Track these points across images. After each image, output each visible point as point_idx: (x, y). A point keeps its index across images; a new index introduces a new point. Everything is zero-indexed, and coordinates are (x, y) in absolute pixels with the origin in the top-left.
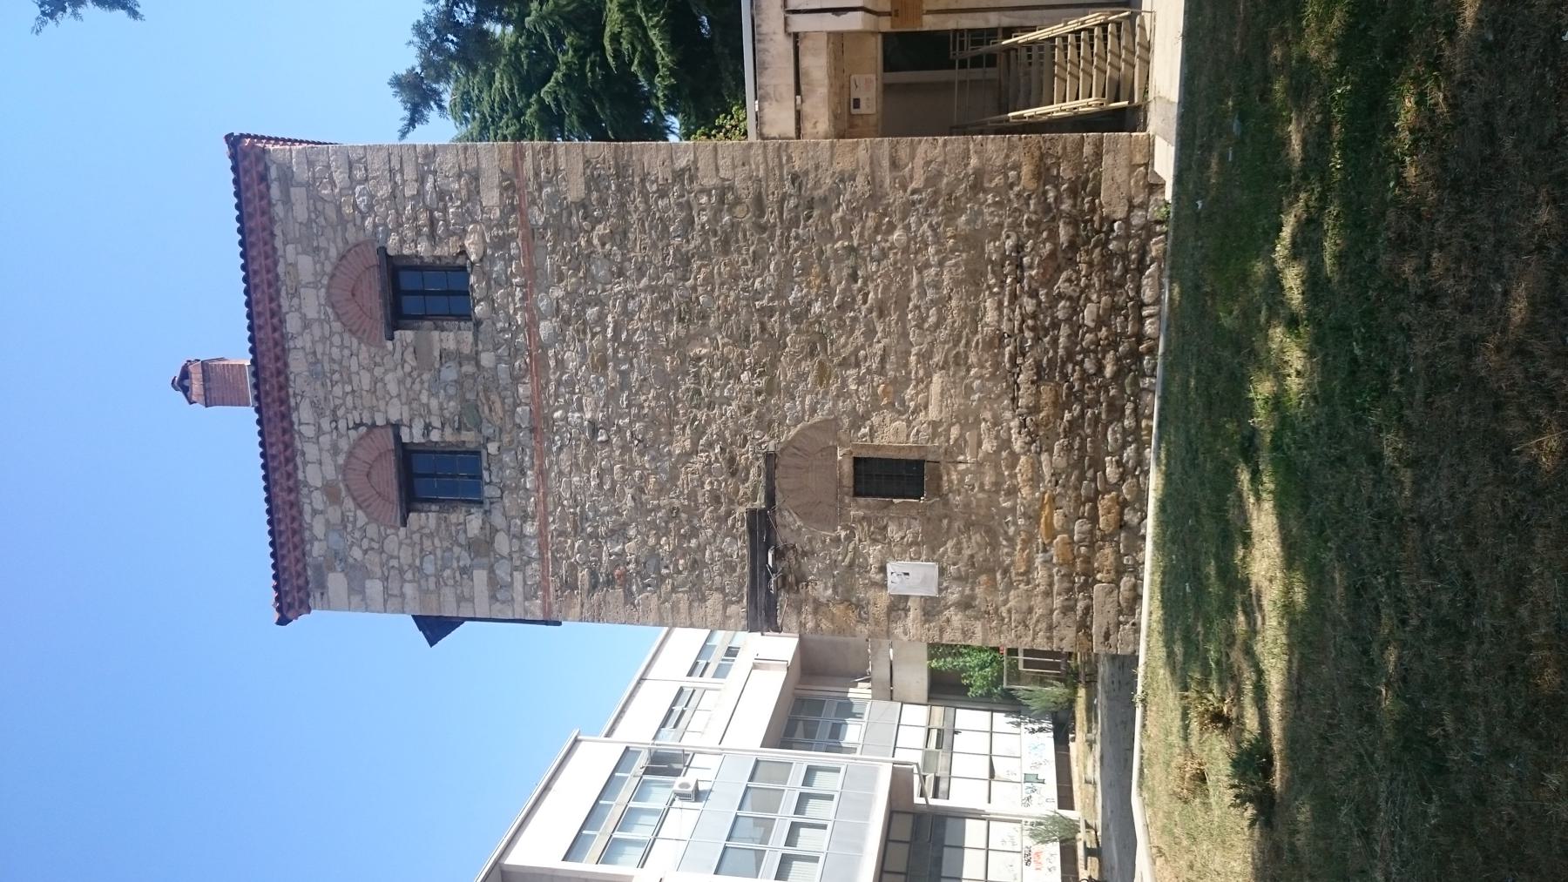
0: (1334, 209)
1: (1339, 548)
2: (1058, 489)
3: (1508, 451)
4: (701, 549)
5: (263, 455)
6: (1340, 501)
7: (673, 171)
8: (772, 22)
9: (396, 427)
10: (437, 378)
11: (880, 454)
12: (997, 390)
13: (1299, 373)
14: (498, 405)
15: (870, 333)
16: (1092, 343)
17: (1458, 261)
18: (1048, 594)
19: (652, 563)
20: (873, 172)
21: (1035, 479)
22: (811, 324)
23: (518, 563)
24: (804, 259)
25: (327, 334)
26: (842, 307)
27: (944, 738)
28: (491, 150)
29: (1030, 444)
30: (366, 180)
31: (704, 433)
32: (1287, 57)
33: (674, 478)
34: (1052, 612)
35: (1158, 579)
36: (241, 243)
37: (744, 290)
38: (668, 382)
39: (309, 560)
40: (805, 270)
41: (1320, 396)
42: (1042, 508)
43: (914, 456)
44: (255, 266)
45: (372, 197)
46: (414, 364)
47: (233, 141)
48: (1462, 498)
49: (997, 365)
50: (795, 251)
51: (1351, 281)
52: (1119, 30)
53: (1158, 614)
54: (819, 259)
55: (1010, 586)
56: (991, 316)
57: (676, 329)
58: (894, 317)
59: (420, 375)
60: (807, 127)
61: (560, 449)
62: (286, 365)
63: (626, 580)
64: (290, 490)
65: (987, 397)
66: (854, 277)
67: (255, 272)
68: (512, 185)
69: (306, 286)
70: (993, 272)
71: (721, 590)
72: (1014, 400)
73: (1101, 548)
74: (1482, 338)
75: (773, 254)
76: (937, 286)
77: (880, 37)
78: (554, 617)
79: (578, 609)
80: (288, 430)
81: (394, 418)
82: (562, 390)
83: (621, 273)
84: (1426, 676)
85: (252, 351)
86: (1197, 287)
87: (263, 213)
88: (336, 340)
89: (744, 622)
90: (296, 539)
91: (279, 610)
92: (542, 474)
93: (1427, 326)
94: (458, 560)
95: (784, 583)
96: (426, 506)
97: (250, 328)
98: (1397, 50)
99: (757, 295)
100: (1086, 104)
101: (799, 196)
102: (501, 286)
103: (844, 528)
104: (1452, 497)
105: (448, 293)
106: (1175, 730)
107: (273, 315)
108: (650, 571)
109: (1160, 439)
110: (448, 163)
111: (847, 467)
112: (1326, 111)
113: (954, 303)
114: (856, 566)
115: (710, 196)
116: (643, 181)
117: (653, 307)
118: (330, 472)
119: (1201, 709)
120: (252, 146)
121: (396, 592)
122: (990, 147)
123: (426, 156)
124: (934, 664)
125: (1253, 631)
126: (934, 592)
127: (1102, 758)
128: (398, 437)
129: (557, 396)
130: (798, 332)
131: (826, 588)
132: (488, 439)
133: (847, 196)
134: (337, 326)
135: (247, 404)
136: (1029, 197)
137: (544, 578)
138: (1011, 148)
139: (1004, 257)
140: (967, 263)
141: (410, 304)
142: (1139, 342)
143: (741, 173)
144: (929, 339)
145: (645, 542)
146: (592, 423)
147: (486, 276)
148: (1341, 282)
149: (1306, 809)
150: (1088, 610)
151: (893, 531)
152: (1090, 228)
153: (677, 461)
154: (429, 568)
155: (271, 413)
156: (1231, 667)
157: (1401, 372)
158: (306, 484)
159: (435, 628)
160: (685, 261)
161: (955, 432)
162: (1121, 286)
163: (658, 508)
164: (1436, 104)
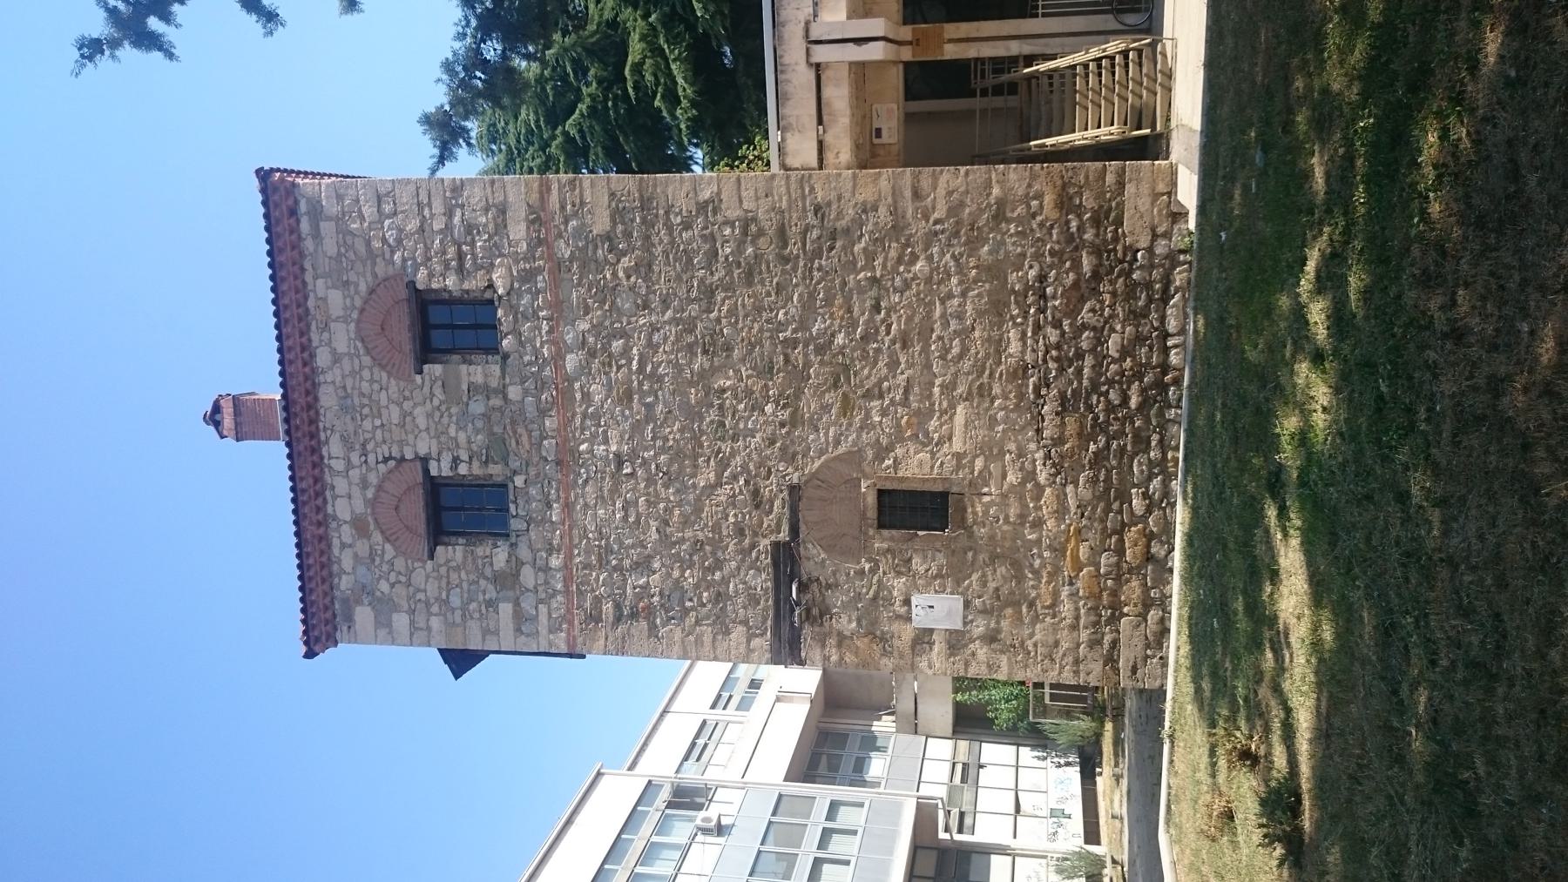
0: (1358, 244)
1: (1367, 586)
2: (1084, 522)
3: (1537, 492)
4: (725, 581)
5: (293, 489)
6: (1368, 539)
7: (697, 203)
8: (794, 52)
9: (425, 461)
10: (465, 413)
11: (904, 486)
12: (1022, 422)
13: (1325, 409)
14: (525, 439)
15: (893, 364)
16: (1117, 373)
17: (1484, 298)
18: (1074, 627)
19: (676, 596)
20: (895, 202)
21: (1061, 511)
22: (834, 356)
23: (543, 596)
24: (827, 290)
26: (865, 338)
27: (969, 772)
28: (517, 183)
29: (1055, 475)
30: (395, 214)
31: (728, 465)
32: (1309, 88)
33: (698, 510)
34: (1078, 645)
35: (1185, 612)
36: (272, 278)
37: (768, 321)
38: (693, 414)
39: (337, 593)
40: (829, 301)
41: (1346, 433)
42: (1068, 540)
43: (939, 488)
44: (286, 301)
45: (400, 230)
46: (442, 397)
47: (263, 175)
48: (1491, 539)
49: (1021, 396)
50: (818, 283)
51: (1376, 317)
52: (1140, 57)
53: (1186, 649)
54: (842, 290)
55: (1036, 619)
56: (1014, 347)
57: (700, 361)
58: (918, 348)
59: (448, 409)
60: (830, 157)
61: (586, 481)
62: (316, 399)
63: (650, 612)
64: (319, 524)
65: (1011, 429)
66: (877, 308)
67: (286, 307)
68: (538, 218)
69: (337, 320)
70: (1017, 302)
71: (745, 622)
72: (1039, 431)
73: (1128, 581)
74: (1509, 378)
75: (797, 285)
76: (960, 316)
77: (901, 67)
78: (578, 650)
79: (602, 642)
80: (318, 464)
81: (422, 452)
82: (588, 422)
83: (646, 306)
84: (1457, 718)
85: (283, 385)
86: (1222, 320)
87: (293, 248)
88: (366, 374)
89: (768, 655)
90: (325, 573)
91: (306, 643)
92: (568, 507)
93: (1454, 364)
94: (484, 592)
95: (807, 616)
96: (453, 539)
97: (281, 362)
98: (1419, 83)
99: (781, 327)
100: (1108, 133)
101: (822, 227)
102: (527, 319)
103: (869, 560)
104: (1481, 537)
105: (476, 327)
106: (1202, 766)
107: (303, 349)
108: (674, 604)
109: (1186, 472)
110: (475, 196)
111: (871, 499)
112: (1349, 143)
113: (977, 334)
114: (880, 599)
115: (733, 227)
116: (667, 213)
117: (677, 340)
118: (359, 506)
119: (1229, 746)
120: (282, 180)
121: (422, 624)
122: (1012, 176)
123: (454, 190)
124: (959, 697)
125: (1280, 669)
126: (959, 626)
127: (1129, 792)
128: (426, 471)
129: (583, 429)
130: (822, 363)
131: (850, 621)
132: (515, 473)
133: (870, 227)
134: (367, 360)
135: (271, 436)
136: (1052, 227)
137: (568, 611)
138: (1034, 177)
139: (1027, 288)
140: (990, 293)
141: (439, 338)
142: (1165, 373)
143: (764, 204)
144: (953, 370)
145: (669, 575)
146: (618, 455)
147: (513, 309)
148: (1366, 318)
149: (1336, 850)
150: (1115, 643)
151: (917, 564)
152: (1113, 258)
153: (702, 494)
154: (456, 601)
155: (301, 448)
156: (1258, 704)
157: (1430, 410)
158: (335, 518)
159: (460, 661)
160: (709, 292)
161: (979, 463)
162: (1146, 316)
163: (683, 540)
164: (1460, 139)
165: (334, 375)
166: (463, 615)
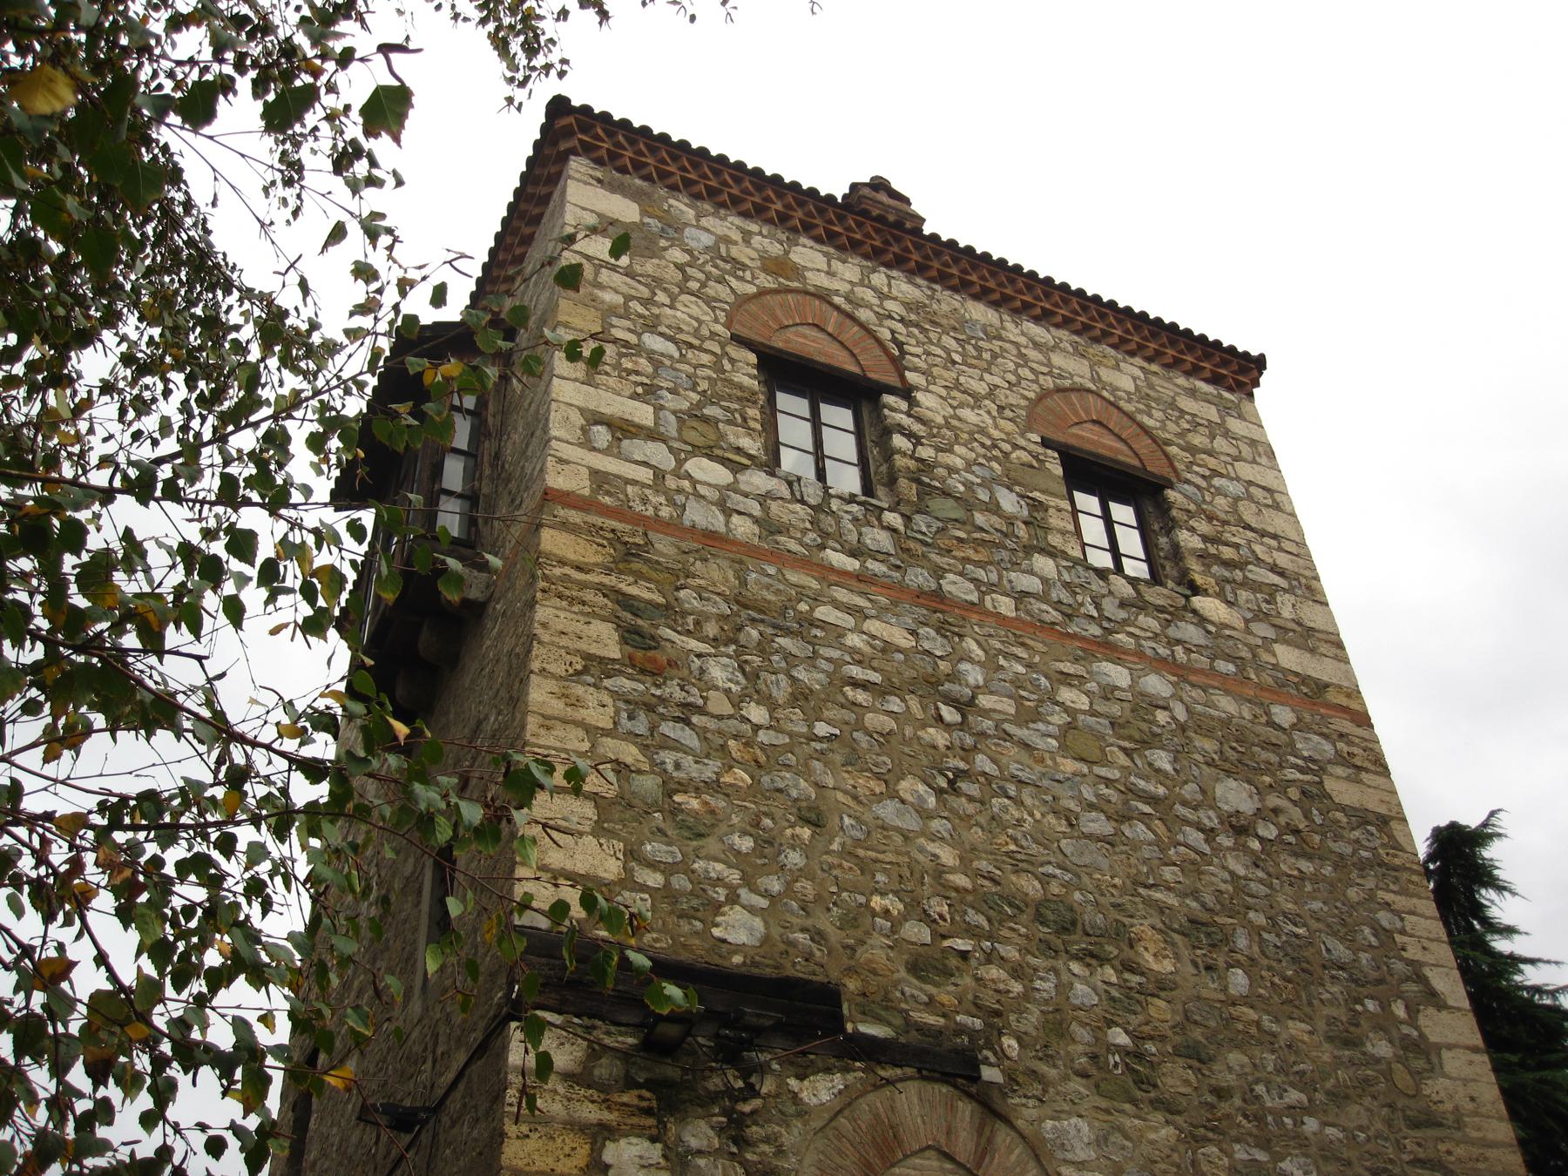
25: (1034, 366)
59: (995, 458)
62: (976, 297)
71: (628, 881)
118: (818, 280)
128: (892, 390)
132: (907, 519)
134: (1049, 383)
154: (654, 342)
165: (1012, 331)
166: (627, 344)
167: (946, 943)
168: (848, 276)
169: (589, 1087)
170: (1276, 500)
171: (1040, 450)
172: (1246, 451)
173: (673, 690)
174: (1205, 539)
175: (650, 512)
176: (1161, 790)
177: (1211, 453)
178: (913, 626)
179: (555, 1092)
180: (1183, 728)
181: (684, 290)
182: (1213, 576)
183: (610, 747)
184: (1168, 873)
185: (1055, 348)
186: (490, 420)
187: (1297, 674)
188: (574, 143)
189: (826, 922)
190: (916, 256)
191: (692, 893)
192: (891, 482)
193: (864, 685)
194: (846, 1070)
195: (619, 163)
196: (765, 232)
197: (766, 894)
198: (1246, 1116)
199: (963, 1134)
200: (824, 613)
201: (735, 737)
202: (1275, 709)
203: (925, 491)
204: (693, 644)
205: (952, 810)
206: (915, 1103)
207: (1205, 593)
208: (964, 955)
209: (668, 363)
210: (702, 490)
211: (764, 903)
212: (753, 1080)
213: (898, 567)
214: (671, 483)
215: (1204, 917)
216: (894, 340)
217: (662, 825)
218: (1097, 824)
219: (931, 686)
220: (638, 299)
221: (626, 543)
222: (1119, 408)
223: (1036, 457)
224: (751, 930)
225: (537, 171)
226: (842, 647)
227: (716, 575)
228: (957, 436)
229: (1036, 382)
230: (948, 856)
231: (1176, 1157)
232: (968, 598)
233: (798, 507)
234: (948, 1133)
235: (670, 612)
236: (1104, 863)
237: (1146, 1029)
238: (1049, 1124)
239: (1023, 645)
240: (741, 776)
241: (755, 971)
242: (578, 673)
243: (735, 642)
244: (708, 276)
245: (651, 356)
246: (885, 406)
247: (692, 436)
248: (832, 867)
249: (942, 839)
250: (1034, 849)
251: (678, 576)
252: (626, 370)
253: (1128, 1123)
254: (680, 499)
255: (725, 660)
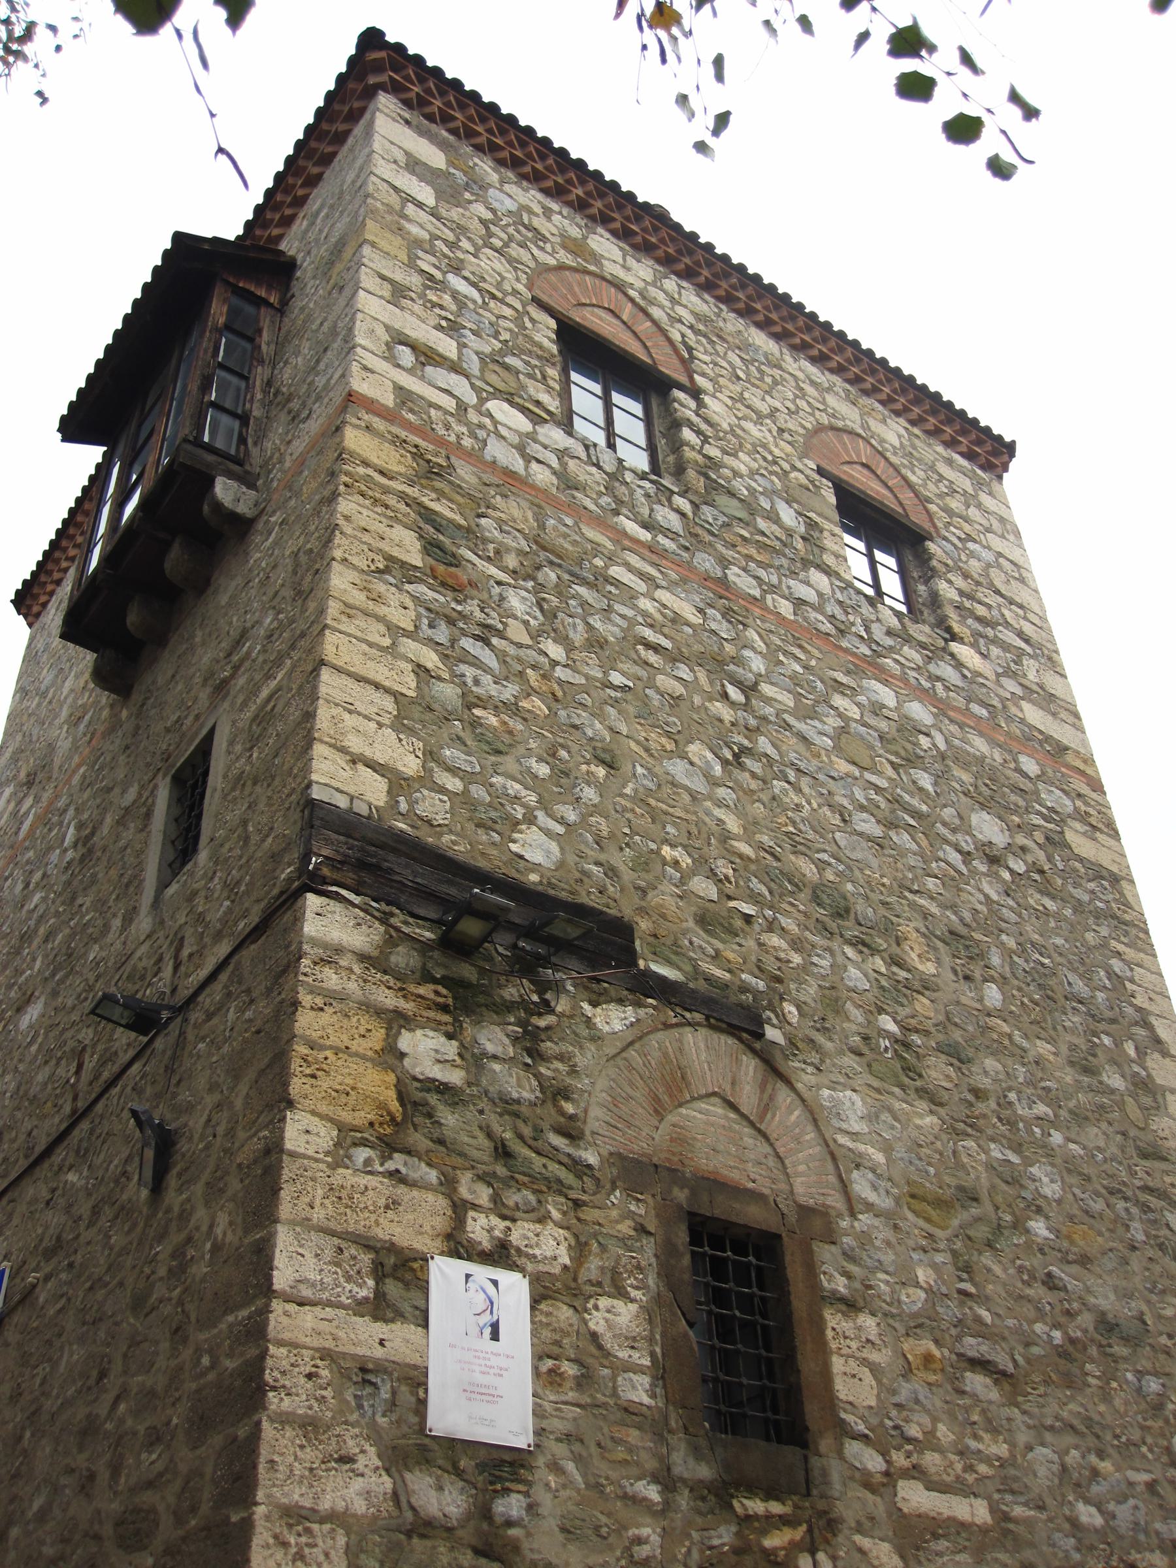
62: (759, 325)
71: (425, 780)
88: (802, 404)
118: (613, 269)
128: (681, 387)
132: (696, 506)
134: (825, 420)
166: (431, 278)
167: (732, 904)
168: (641, 274)
169: (385, 972)
170: (1020, 574)
171: (817, 477)
172: (996, 525)
173: (472, 607)
174: (961, 593)
175: (453, 438)
176: (924, 808)
177: (966, 520)
178: (702, 605)
179: (351, 970)
180: (943, 757)
181: (488, 245)
182: (969, 627)
183: (409, 647)
184: (931, 883)
185: (829, 390)
186: (264, 347)
187: (1041, 732)
188: (383, 78)
189: (621, 860)
190: (705, 272)
191: (490, 805)
192: (679, 471)
193: (656, 648)
194: (638, 1004)
195: (427, 110)
196: (565, 213)
197: (562, 821)
198: (1000, 1119)
199: (748, 1087)
200: (616, 571)
201: (534, 667)
202: (1023, 759)
203: (713, 486)
204: (493, 571)
205: (736, 781)
206: (701, 1049)
207: (961, 641)
208: (748, 919)
209: (471, 306)
210: (504, 431)
211: (560, 829)
212: (548, 996)
213: (687, 549)
214: (473, 416)
215: (963, 931)
216: (684, 343)
217: (462, 734)
218: (867, 824)
219: (717, 664)
220: (445, 241)
221: (429, 461)
222: (886, 459)
223: (812, 482)
224: (548, 853)
225: (325, 126)
226: (635, 607)
227: (516, 513)
228: (741, 445)
229: (813, 415)
230: (733, 824)
231: (939, 1144)
232: (752, 592)
233: (594, 470)
234: (733, 1083)
235: (471, 534)
236: (875, 863)
237: (913, 1022)
238: (826, 1093)
239: (800, 647)
240: (537, 705)
241: (552, 892)
242: (379, 571)
243: (534, 579)
244: (511, 238)
245: (455, 295)
246: (675, 400)
247: (493, 379)
248: (625, 809)
249: (728, 806)
250: (811, 835)
251: (479, 506)
252: (430, 301)
253: (897, 1105)
254: (481, 434)
255: (524, 594)
